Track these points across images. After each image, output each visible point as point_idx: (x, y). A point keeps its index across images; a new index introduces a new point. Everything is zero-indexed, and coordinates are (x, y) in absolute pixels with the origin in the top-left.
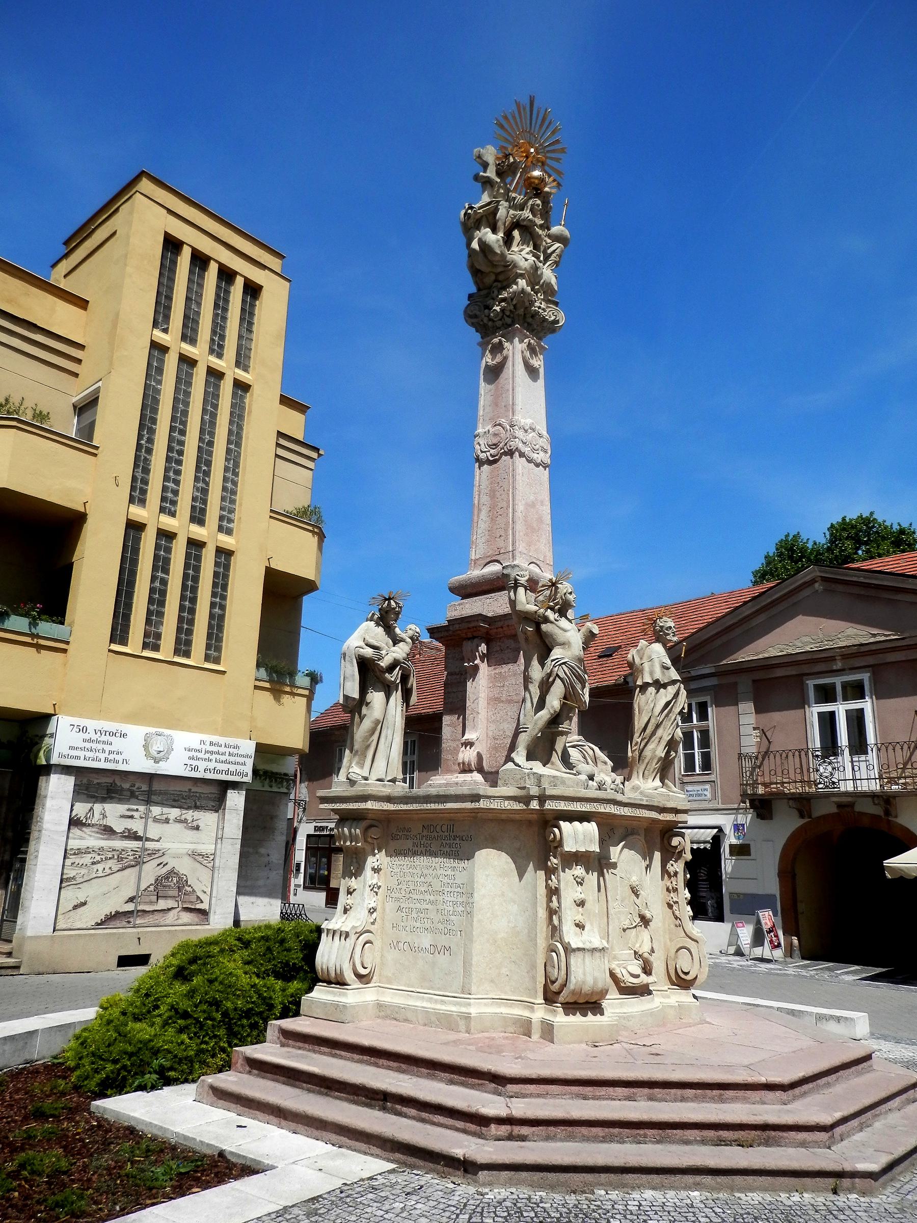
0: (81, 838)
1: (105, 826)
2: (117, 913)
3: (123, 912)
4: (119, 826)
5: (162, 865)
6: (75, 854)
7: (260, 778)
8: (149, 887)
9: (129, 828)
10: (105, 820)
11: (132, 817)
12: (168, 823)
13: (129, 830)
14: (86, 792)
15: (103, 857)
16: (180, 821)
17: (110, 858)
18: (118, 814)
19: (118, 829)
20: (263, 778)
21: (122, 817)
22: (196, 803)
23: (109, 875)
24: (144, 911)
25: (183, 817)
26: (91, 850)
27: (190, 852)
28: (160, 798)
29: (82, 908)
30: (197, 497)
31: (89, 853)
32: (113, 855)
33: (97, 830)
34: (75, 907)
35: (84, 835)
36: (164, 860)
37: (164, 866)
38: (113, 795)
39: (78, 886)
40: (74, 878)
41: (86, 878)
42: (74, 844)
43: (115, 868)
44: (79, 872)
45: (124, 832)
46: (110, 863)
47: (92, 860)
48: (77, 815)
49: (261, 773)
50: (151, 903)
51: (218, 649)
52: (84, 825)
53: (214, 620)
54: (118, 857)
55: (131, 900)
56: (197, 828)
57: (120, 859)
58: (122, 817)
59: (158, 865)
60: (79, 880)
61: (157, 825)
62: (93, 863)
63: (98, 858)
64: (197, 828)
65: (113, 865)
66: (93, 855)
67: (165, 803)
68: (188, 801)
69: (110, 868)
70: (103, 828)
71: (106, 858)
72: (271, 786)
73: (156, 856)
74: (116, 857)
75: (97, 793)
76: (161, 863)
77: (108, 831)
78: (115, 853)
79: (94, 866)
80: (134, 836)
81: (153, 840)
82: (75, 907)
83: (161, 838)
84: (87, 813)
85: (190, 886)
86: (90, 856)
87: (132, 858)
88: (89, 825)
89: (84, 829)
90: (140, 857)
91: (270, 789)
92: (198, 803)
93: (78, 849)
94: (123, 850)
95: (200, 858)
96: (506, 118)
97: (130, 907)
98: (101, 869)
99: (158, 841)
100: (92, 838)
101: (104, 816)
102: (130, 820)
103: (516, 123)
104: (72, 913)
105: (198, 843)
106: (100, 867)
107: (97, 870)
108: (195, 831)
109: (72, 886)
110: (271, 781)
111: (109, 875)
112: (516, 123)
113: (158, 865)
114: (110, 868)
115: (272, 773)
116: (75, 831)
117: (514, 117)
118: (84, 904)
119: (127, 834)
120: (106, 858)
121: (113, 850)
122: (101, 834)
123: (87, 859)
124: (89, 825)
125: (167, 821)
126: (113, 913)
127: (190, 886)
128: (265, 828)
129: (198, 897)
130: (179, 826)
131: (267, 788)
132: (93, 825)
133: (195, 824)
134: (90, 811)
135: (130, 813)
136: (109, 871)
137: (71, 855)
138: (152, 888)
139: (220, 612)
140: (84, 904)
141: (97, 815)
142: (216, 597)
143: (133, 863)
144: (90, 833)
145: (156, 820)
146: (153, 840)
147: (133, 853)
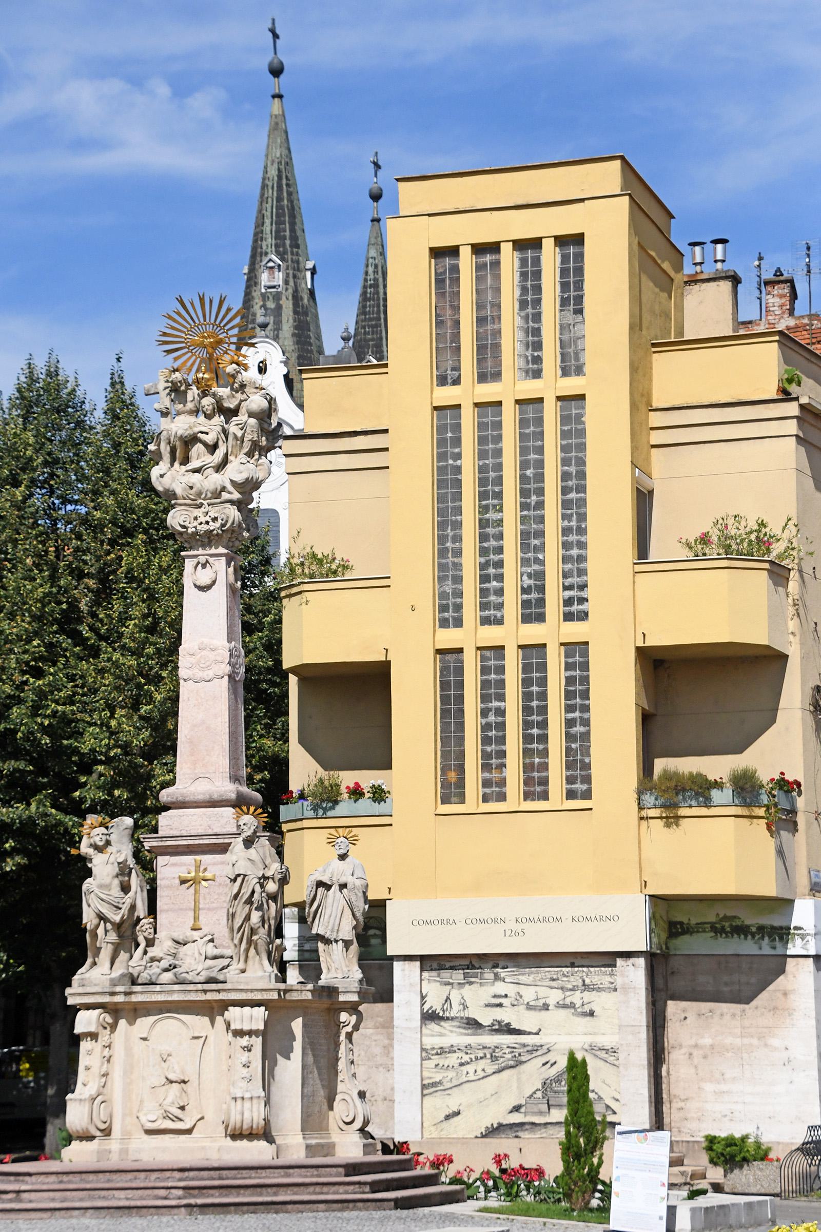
0: (441, 1035)
1: (468, 1018)
2: (500, 1125)
3: (507, 1125)
4: (485, 1018)
5: (548, 1065)
6: (437, 1054)
7: (753, 937)
8: (535, 1093)
9: (499, 1019)
10: (466, 1011)
11: (500, 1005)
12: (547, 1009)
13: (499, 1023)
14: (438, 979)
15: (473, 1057)
16: (565, 1006)
17: (481, 1058)
18: (482, 1003)
19: (485, 1021)
20: (757, 937)
21: (487, 1006)
22: (584, 981)
23: (483, 1078)
24: (533, 1124)
25: (568, 1001)
26: (455, 1049)
27: (586, 1047)
28: (531, 978)
29: (456, 1119)
30: (530, 587)
31: (455, 1052)
32: (485, 1054)
33: (458, 1024)
34: (448, 1117)
35: (443, 1031)
36: (551, 1057)
37: (552, 1065)
38: (473, 980)
39: (447, 1092)
40: (440, 1083)
41: (455, 1083)
42: (429, 1042)
43: (490, 1070)
44: (445, 1075)
45: (493, 1025)
46: (482, 1064)
47: (459, 1061)
48: (431, 1007)
49: (754, 929)
50: (541, 1113)
51: (587, 780)
52: (442, 1019)
53: (575, 742)
54: (492, 1056)
55: (517, 1109)
56: (591, 1014)
57: (494, 1059)
58: (487, 1006)
59: (544, 1065)
60: (449, 1085)
61: (532, 1013)
62: (462, 1064)
63: (466, 1058)
64: (591, 1014)
65: (487, 1065)
66: (460, 1054)
67: (539, 983)
68: (572, 979)
69: (483, 1070)
70: (465, 1021)
71: (477, 1059)
72: (774, 948)
73: (539, 1053)
74: (488, 1056)
75: (451, 978)
76: (547, 1062)
77: (473, 1025)
78: (486, 1051)
79: (463, 1068)
80: (508, 1029)
81: (530, 1033)
82: (448, 1117)
83: (540, 1030)
84: (444, 1005)
85: (593, 1091)
86: (456, 1055)
87: (509, 1056)
88: (448, 1019)
89: (442, 1023)
90: (520, 1055)
91: (773, 952)
92: (587, 981)
93: (441, 1048)
94: (497, 1047)
95: (603, 1054)
96: (165, 334)
97: (517, 1118)
98: (471, 1072)
99: (537, 1034)
100: (454, 1034)
101: (465, 1007)
102: (498, 1009)
103: (192, 318)
104: (446, 1124)
105: (595, 1034)
106: (470, 1068)
107: (467, 1073)
108: (588, 1018)
109: (439, 1093)
110: (774, 940)
111: (483, 1078)
112: (192, 318)
113: (544, 1065)
114: (483, 1070)
115: (773, 928)
116: (433, 1026)
117: (173, 328)
118: (458, 1113)
119: (497, 1027)
120: (477, 1059)
121: (484, 1048)
122: (464, 1028)
123: (453, 1059)
124: (448, 1019)
125: (546, 1007)
126: (495, 1126)
127: (593, 1091)
128: (775, 1009)
129: (608, 1107)
130: (563, 1013)
131: (767, 950)
132: (452, 1019)
133: (587, 1008)
134: (446, 1001)
135: (497, 1001)
136: (482, 1074)
137: (432, 1055)
138: (539, 1094)
139: (583, 729)
140: (458, 1113)
141: (456, 1007)
142: (574, 712)
143: (512, 1063)
144: (451, 1028)
145: (529, 1007)
146: (530, 1033)
147: (510, 1050)
